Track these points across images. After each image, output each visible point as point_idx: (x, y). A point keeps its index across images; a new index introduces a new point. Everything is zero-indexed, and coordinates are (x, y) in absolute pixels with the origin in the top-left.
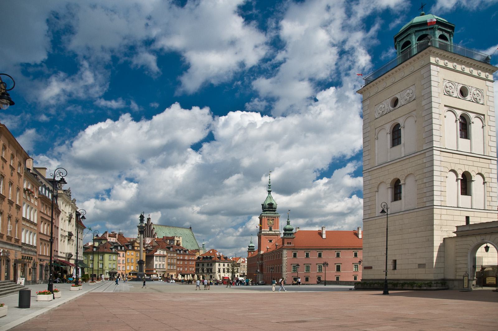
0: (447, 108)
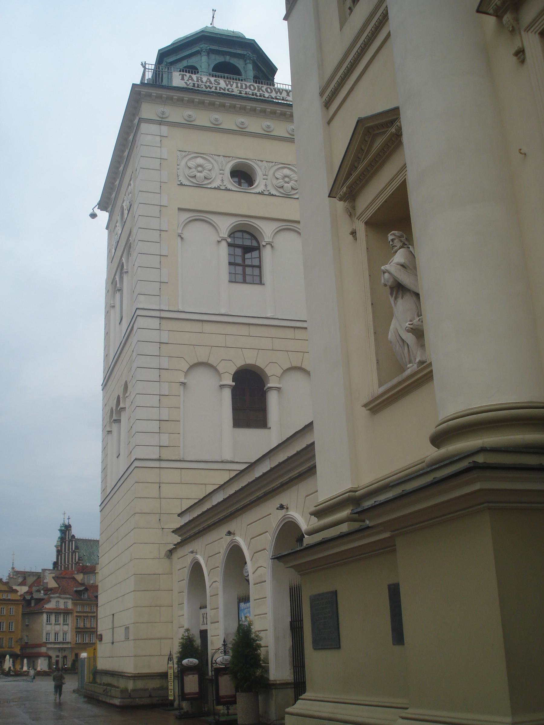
0: (186, 216)
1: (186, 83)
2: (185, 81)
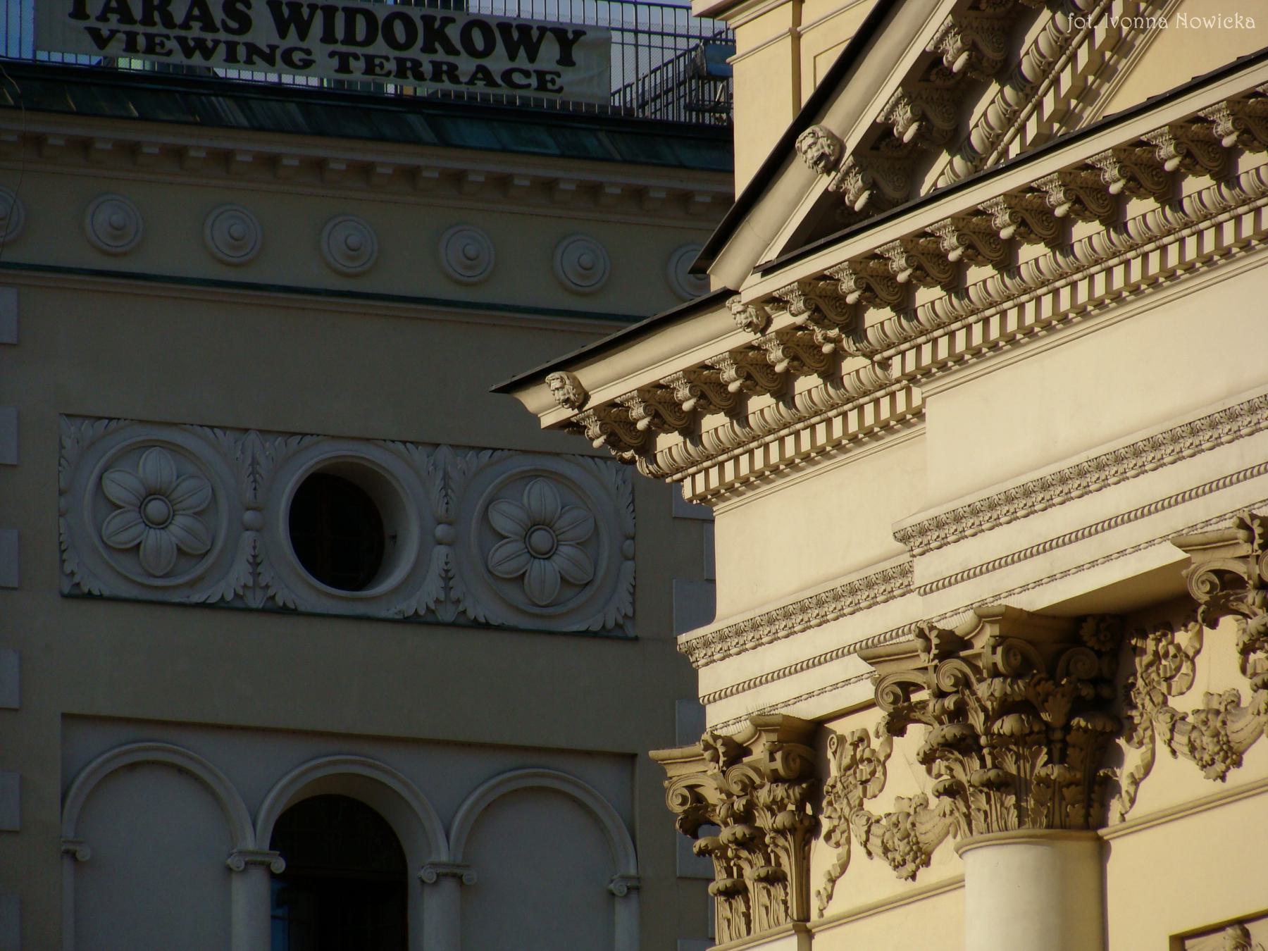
1: (95, 33)
2: (92, 23)
